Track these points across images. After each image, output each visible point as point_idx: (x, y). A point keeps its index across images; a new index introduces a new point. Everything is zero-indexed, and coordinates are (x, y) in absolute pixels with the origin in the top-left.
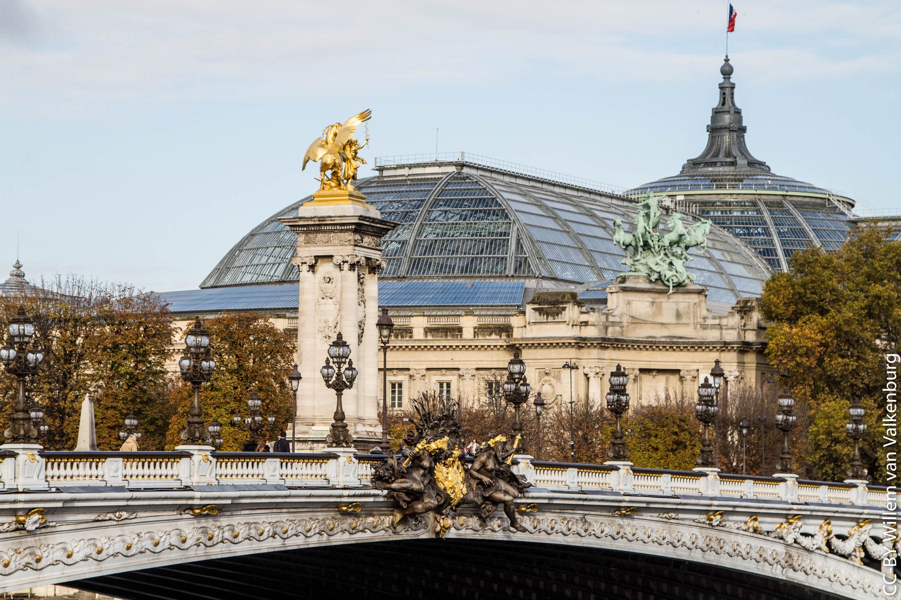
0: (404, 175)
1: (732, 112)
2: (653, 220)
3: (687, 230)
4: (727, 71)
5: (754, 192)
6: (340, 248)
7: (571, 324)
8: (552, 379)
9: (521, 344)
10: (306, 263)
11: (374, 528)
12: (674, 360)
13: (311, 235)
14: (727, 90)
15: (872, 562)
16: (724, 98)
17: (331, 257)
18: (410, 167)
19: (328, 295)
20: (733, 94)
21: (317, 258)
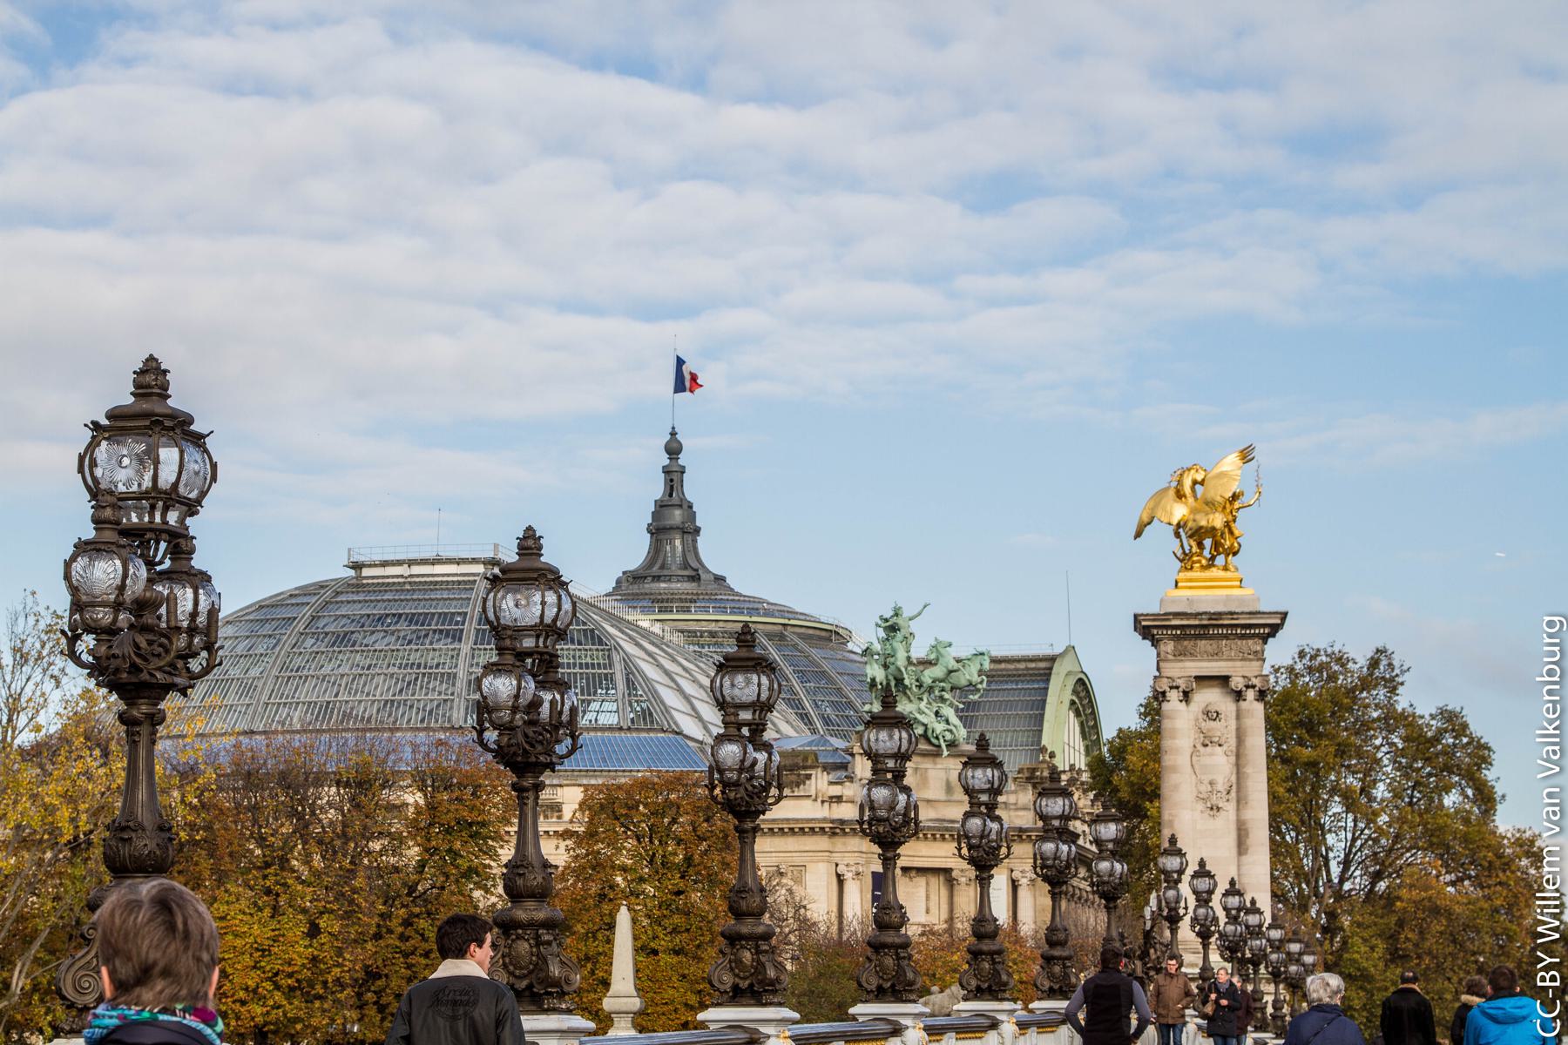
0: (402, 576)
1: (685, 506)
4: (673, 449)
6: (1239, 664)
7: (819, 800)
10: (1177, 687)
12: (943, 854)
13: (1186, 643)
14: (673, 476)
16: (672, 487)
18: (411, 563)
19: (1216, 739)
20: (682, 481)
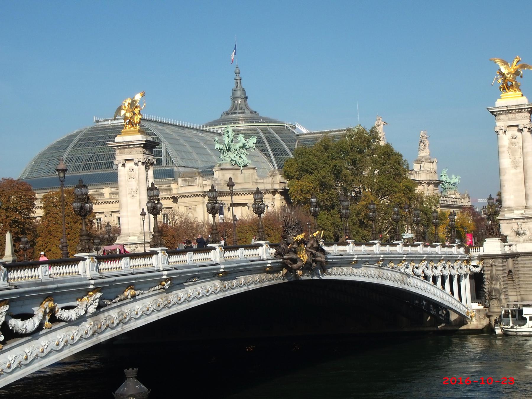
1: (241, 90)
2: (231, 137)
3: (247, 141)
5: (255, 124)
6: (136, 155)
7: (199, 186)
8: (192, 211)
9: (177, 196)
11: (277, 278)
14: (238, 81)
15: (426, 277)
17: (132, 160)
19: (132, 177)
21: (126, 160)
